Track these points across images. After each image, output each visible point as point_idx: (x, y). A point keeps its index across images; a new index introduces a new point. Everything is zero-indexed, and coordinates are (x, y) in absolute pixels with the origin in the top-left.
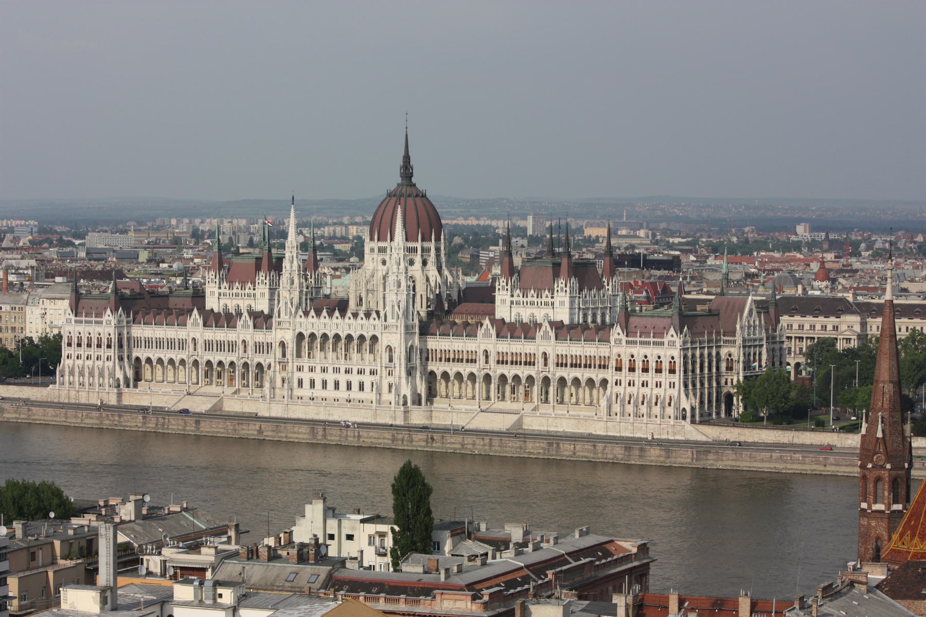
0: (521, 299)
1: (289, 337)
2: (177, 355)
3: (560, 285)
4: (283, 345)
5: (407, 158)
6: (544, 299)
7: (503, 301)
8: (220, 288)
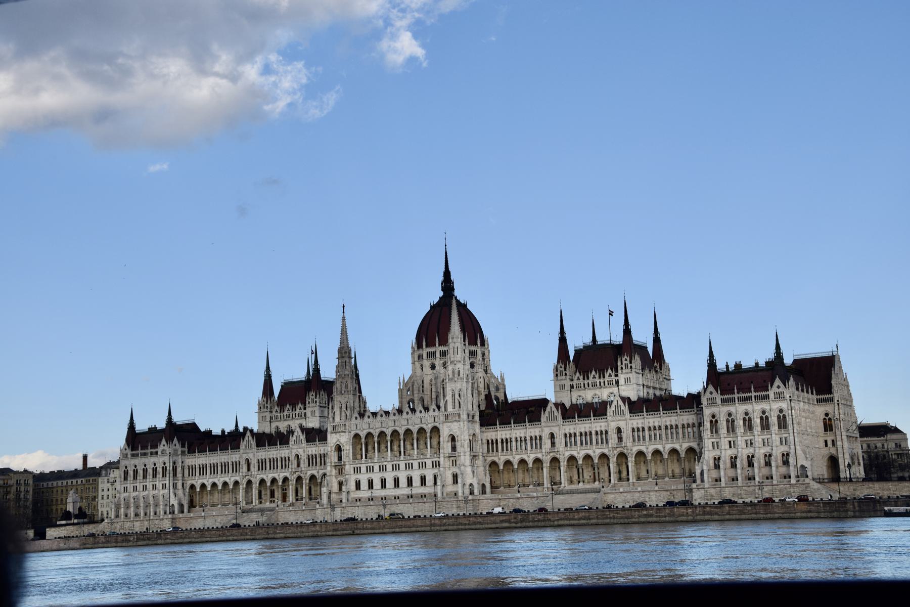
0: (581, 381)
1: (345, 439)
2: (230, 479)
4: (339, 449)
5: (447, 274)
7: (562, 387)
8: (271, 412)
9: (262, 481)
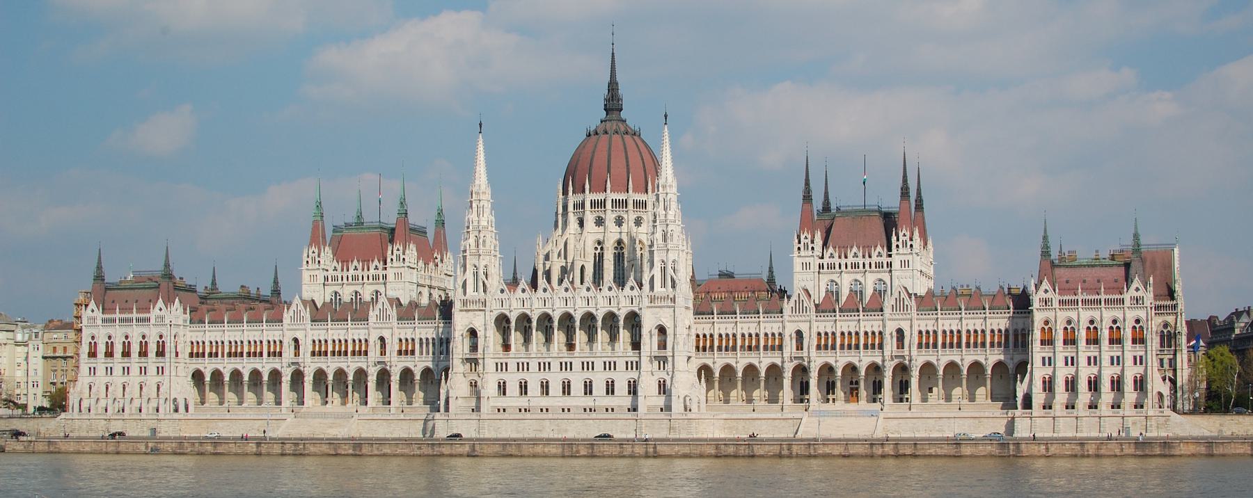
0: (836, 260)
1: (484, 324)
2: (265, 366)
3: (901, 238)
4: (473, 333)
5: (613, 86)
6: (875, 259)
7: (806, 266)
9: (320, 375)
